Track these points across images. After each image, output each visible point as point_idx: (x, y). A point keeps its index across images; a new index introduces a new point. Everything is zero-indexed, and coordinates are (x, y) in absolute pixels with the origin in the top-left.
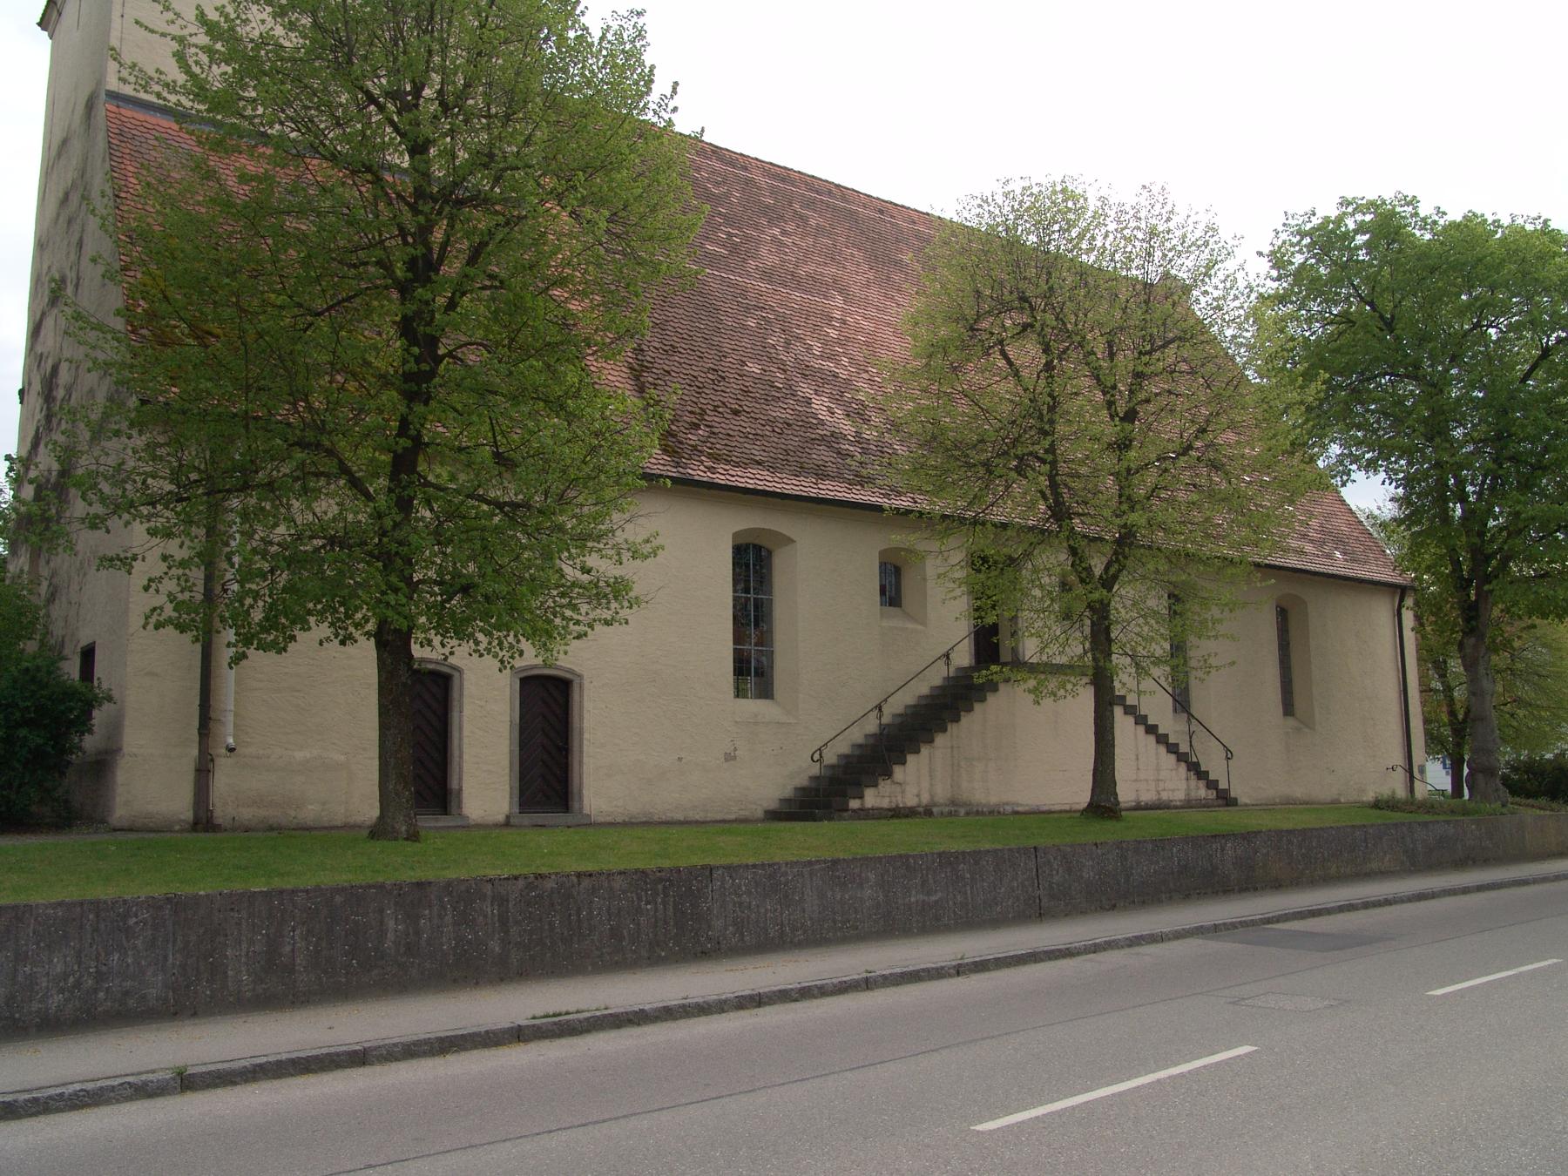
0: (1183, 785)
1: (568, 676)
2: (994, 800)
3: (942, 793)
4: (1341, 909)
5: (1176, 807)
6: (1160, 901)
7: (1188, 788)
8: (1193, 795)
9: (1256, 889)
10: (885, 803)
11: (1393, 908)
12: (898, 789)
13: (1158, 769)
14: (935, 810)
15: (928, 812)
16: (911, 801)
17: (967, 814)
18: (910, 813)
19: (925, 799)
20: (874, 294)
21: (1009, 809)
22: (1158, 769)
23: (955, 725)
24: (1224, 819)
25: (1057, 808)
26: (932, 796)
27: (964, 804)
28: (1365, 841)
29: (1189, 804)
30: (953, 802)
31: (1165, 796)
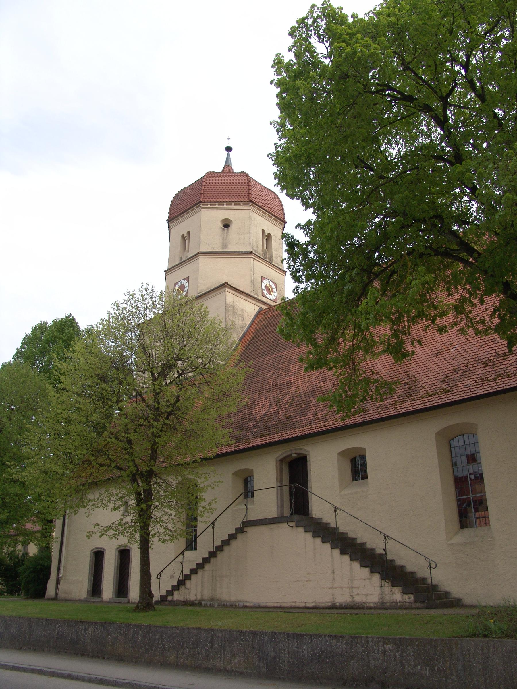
0: (377, 591)
1: (102, 550)
2: (233, 599)
3: (207, 594)
4: (33, 671)
5: (239, 607)
6: (43, 651)
7: (382, 593)
8: (387, 599)
9: (104, 658)
10: (182, 598)
11: (72, 682)
12: (187, 591)
13: (352, 580)
14: (203, 603)
15: (200, 604)
16: (192, 598)
17: (219, 606)
18: (192, 604)
19: (199, 597)
20: (127, 353)
21: (241, 604)
22: (352, 580)
23: (215, 559)
24: (431, 624)
25: (271, 605)
26: (202, 596)
27: (218, 600)
28: (212, 641)
29: (382, 606)
30: (212, 599)
31: (358, 599)
